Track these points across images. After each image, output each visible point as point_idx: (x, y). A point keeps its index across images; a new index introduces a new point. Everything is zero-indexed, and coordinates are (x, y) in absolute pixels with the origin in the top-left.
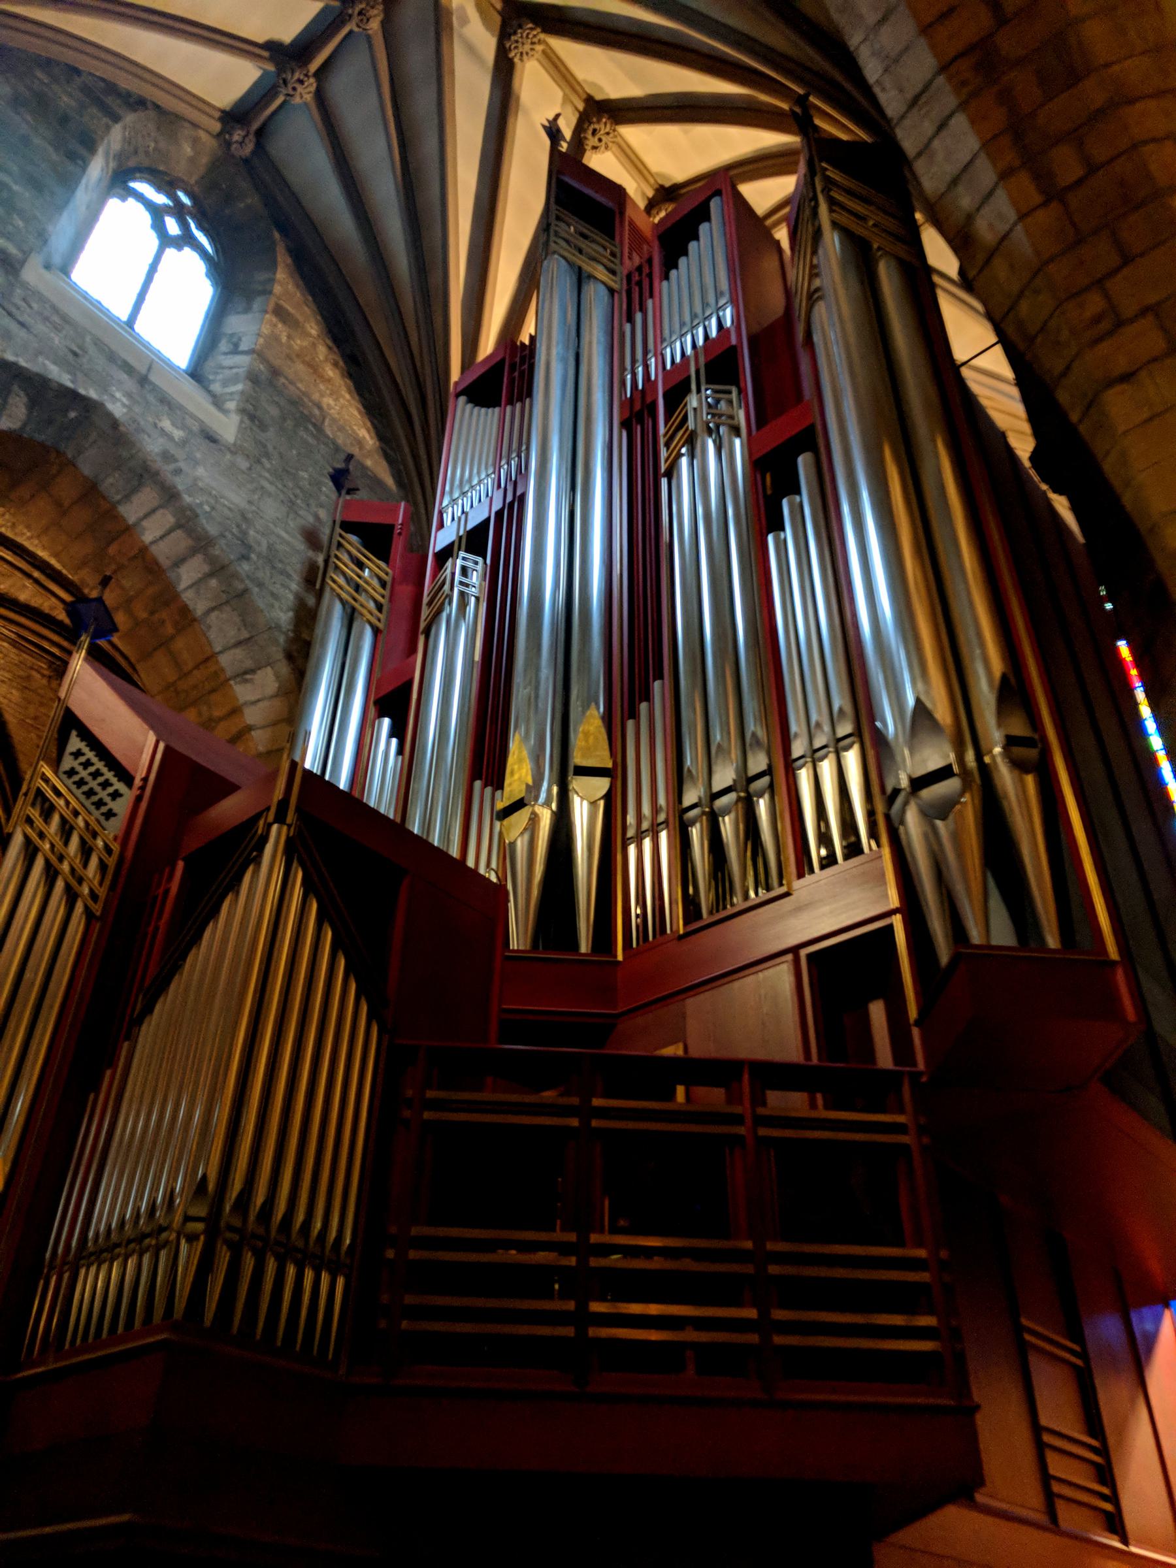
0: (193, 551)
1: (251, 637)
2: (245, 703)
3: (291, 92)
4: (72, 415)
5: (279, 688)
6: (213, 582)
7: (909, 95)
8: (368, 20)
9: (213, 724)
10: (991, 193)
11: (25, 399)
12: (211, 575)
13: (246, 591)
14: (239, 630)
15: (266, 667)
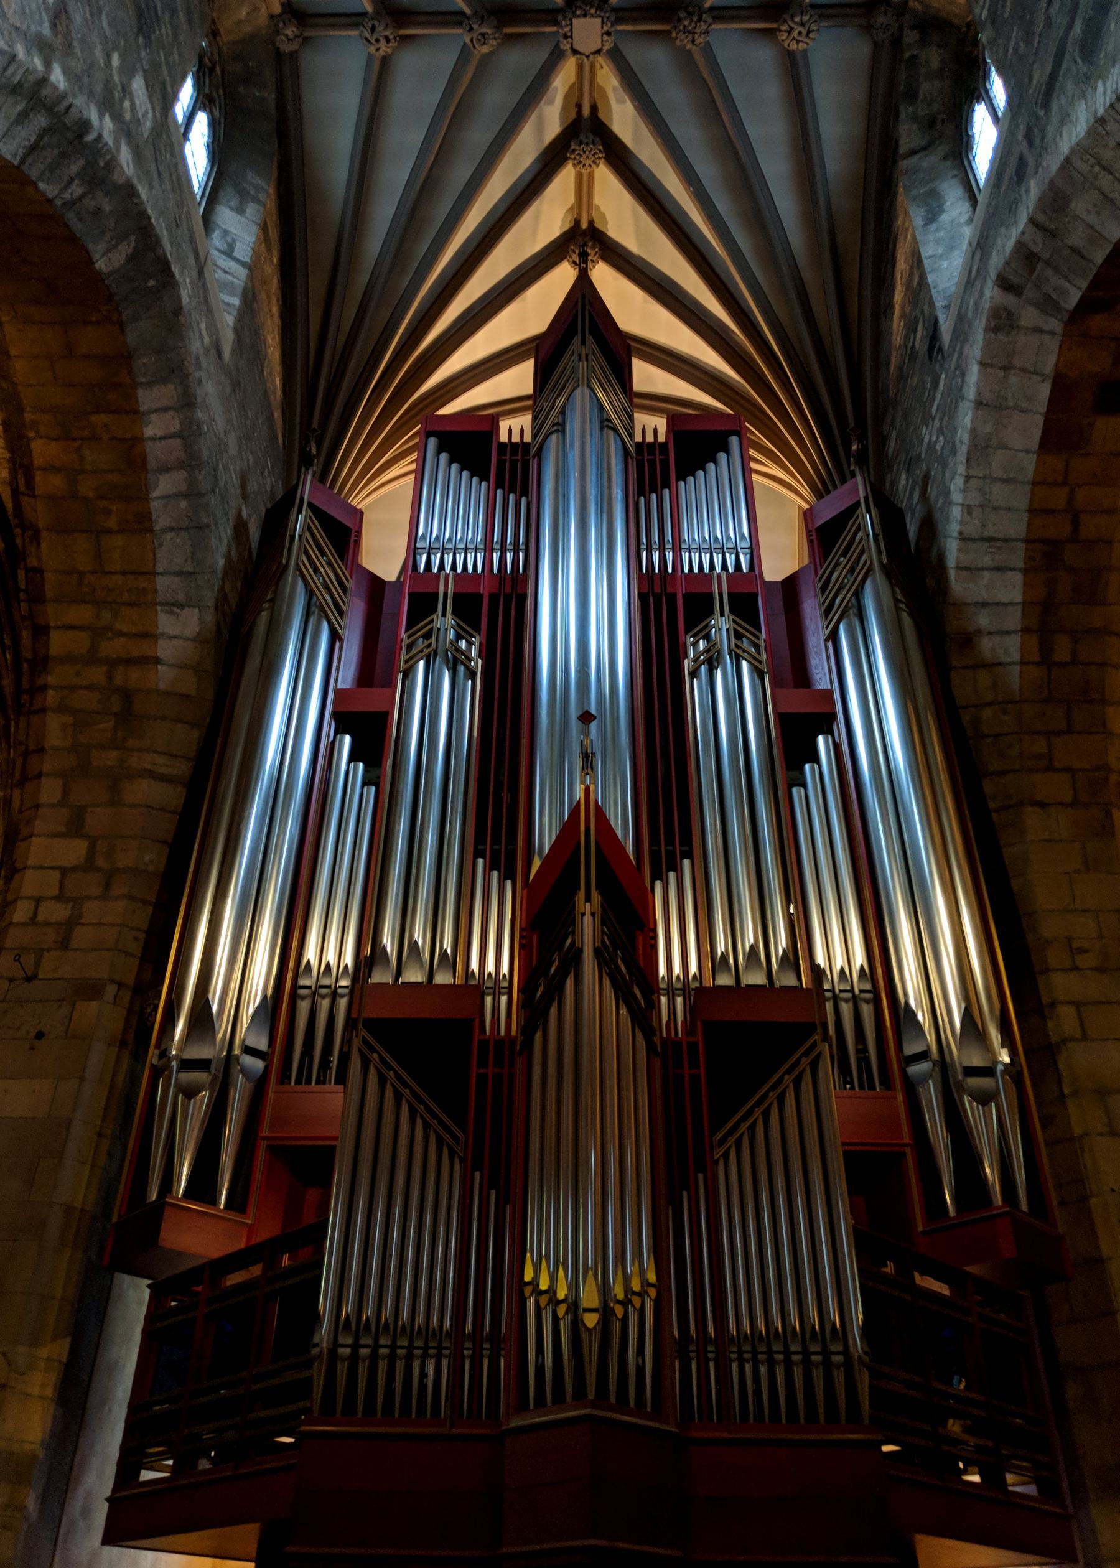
0: (181, 465)
1: (194, 573)
2: (162, 634)
3: (373, 41)
4: (152, 283)
5: (198, 634)
6: (183, 504)
7: (986, 534)
8: (484, 43)
9: (110, 634)
10: (1008, 633)
11: (130, 251)
12: (185, 496)
13: (208, 526)
14: (186, 560)
15: (194, 607)
